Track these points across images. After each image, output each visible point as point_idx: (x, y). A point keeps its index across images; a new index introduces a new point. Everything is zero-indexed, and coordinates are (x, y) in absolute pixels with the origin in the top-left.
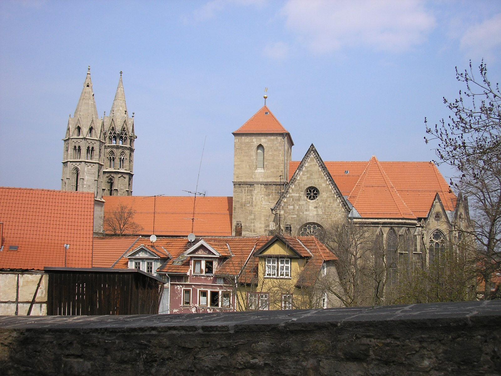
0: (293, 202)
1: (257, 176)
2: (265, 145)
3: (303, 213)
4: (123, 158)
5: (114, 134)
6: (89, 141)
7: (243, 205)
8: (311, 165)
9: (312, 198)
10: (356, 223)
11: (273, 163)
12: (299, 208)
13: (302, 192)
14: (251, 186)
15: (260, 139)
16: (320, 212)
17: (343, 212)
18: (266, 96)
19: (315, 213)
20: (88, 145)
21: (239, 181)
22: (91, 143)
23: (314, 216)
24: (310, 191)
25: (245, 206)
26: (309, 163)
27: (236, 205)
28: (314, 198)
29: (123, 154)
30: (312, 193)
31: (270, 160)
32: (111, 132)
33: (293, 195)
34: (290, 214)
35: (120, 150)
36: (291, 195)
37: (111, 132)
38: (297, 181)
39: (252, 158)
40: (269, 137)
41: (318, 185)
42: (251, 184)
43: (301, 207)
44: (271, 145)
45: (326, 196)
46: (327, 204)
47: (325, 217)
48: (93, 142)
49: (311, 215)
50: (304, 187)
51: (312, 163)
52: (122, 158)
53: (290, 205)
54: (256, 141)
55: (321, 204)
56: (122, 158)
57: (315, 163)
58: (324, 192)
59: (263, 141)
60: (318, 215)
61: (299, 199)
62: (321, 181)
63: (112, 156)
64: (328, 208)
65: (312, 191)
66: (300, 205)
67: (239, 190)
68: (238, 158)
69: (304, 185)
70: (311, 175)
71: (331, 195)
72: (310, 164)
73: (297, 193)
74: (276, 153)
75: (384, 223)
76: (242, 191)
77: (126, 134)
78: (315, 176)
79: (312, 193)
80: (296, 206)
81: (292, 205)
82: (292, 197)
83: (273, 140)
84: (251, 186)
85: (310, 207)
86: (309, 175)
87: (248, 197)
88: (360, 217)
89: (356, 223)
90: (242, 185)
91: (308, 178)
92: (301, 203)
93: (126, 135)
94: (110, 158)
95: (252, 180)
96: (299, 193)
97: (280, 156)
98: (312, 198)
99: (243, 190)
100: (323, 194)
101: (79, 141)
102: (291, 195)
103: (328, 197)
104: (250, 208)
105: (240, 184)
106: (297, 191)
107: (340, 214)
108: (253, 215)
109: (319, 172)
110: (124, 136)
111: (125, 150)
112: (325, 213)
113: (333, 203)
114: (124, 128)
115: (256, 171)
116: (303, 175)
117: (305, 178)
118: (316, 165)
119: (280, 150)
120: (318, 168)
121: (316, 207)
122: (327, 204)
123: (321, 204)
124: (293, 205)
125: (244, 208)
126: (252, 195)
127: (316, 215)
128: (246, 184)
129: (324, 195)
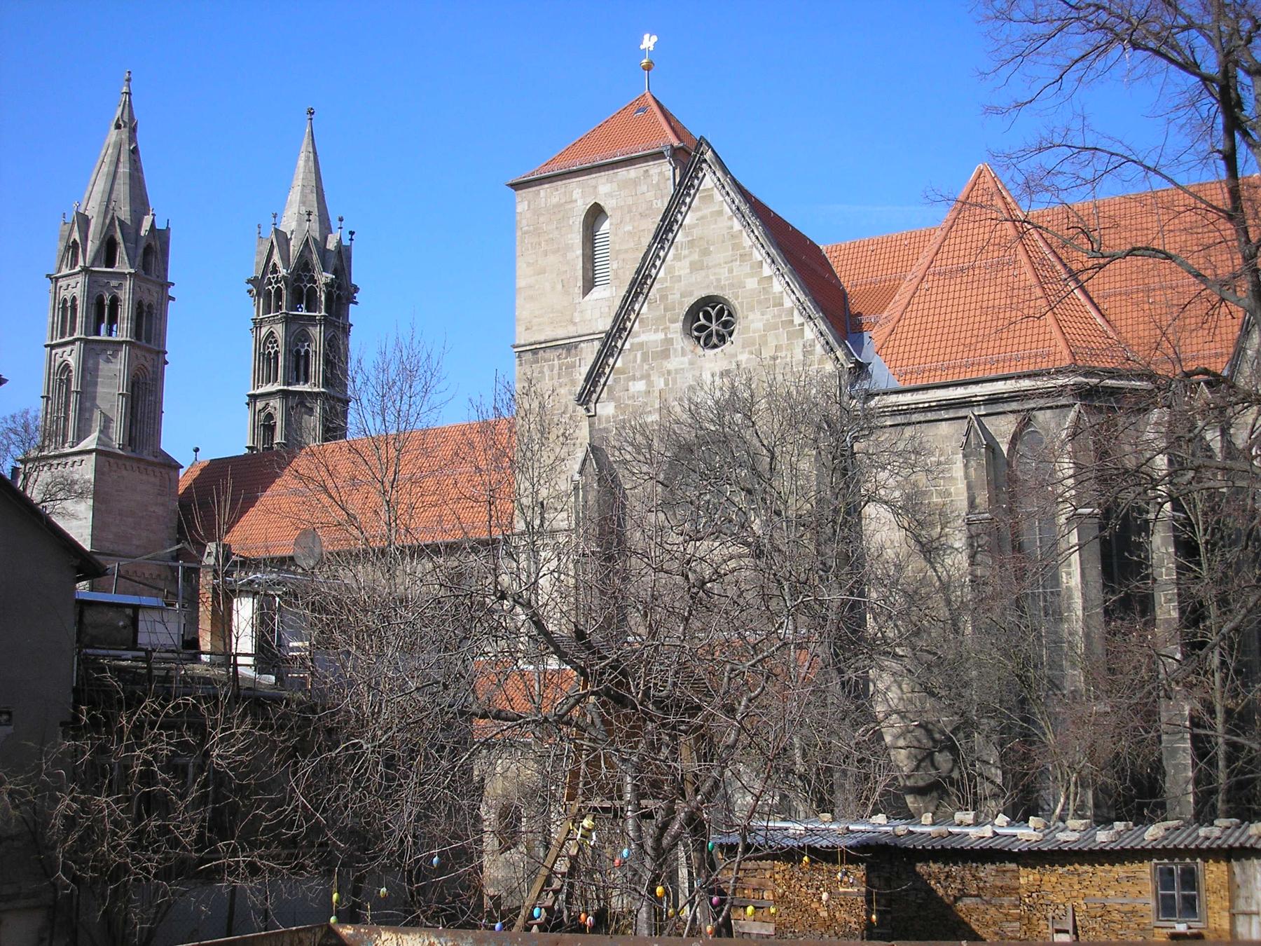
0: (646, 367)
1: (588, 315)
2: (607, 205)
8: (702, 218)
9: (715, 340)
10: (882, 415)
12: (667, 384)
14: (569, 350)
15: (595, 187)
21: (532, 340)
24: (708, 317)
26: (698, 209)
28: (722, 339)
31: (626, 251)
33: (643, 338)
36: (636, 340)
39: (570, 256)
40: (623, 173)
41: (732, 285)
44: (630, 201)
45: (760, 325)
50: (681, 303)
51: (707, 211)
52: (303, 351)
53: (634, 378)
56: (303, 351)
57: (716, 208)
58: (752, 309)
59: (604, 188)
61: (665, 354)
62: (741, 270)
65: (713, 314)
66: (669, 372)
68: (529, 264)
69: (682, 296)
70: (705, 252)
71: (780, 316)
72: (699, 214)
73: (656, 331)
75: (993, 400)
78: (720, 255)
81: (642, 378)
82: (641, 345)
83: (635, 182)
84: (569, 350)
86: (696, 257)
88: (900, 385)
90: (541, 352)
91: (695, 267)
92: (673, 363)
93: (315, 282)
95: (572, 331)
96: (666, 329)
98: (715, 340)
99: (546, 369)
101: (72, 282)
102: (636, 340)
103: (769, 327)
115: (587, 297)
118: (720, 213)
120: (729, 223)
124: (647, 377)
128: (552, 346)
129: (751, 321)
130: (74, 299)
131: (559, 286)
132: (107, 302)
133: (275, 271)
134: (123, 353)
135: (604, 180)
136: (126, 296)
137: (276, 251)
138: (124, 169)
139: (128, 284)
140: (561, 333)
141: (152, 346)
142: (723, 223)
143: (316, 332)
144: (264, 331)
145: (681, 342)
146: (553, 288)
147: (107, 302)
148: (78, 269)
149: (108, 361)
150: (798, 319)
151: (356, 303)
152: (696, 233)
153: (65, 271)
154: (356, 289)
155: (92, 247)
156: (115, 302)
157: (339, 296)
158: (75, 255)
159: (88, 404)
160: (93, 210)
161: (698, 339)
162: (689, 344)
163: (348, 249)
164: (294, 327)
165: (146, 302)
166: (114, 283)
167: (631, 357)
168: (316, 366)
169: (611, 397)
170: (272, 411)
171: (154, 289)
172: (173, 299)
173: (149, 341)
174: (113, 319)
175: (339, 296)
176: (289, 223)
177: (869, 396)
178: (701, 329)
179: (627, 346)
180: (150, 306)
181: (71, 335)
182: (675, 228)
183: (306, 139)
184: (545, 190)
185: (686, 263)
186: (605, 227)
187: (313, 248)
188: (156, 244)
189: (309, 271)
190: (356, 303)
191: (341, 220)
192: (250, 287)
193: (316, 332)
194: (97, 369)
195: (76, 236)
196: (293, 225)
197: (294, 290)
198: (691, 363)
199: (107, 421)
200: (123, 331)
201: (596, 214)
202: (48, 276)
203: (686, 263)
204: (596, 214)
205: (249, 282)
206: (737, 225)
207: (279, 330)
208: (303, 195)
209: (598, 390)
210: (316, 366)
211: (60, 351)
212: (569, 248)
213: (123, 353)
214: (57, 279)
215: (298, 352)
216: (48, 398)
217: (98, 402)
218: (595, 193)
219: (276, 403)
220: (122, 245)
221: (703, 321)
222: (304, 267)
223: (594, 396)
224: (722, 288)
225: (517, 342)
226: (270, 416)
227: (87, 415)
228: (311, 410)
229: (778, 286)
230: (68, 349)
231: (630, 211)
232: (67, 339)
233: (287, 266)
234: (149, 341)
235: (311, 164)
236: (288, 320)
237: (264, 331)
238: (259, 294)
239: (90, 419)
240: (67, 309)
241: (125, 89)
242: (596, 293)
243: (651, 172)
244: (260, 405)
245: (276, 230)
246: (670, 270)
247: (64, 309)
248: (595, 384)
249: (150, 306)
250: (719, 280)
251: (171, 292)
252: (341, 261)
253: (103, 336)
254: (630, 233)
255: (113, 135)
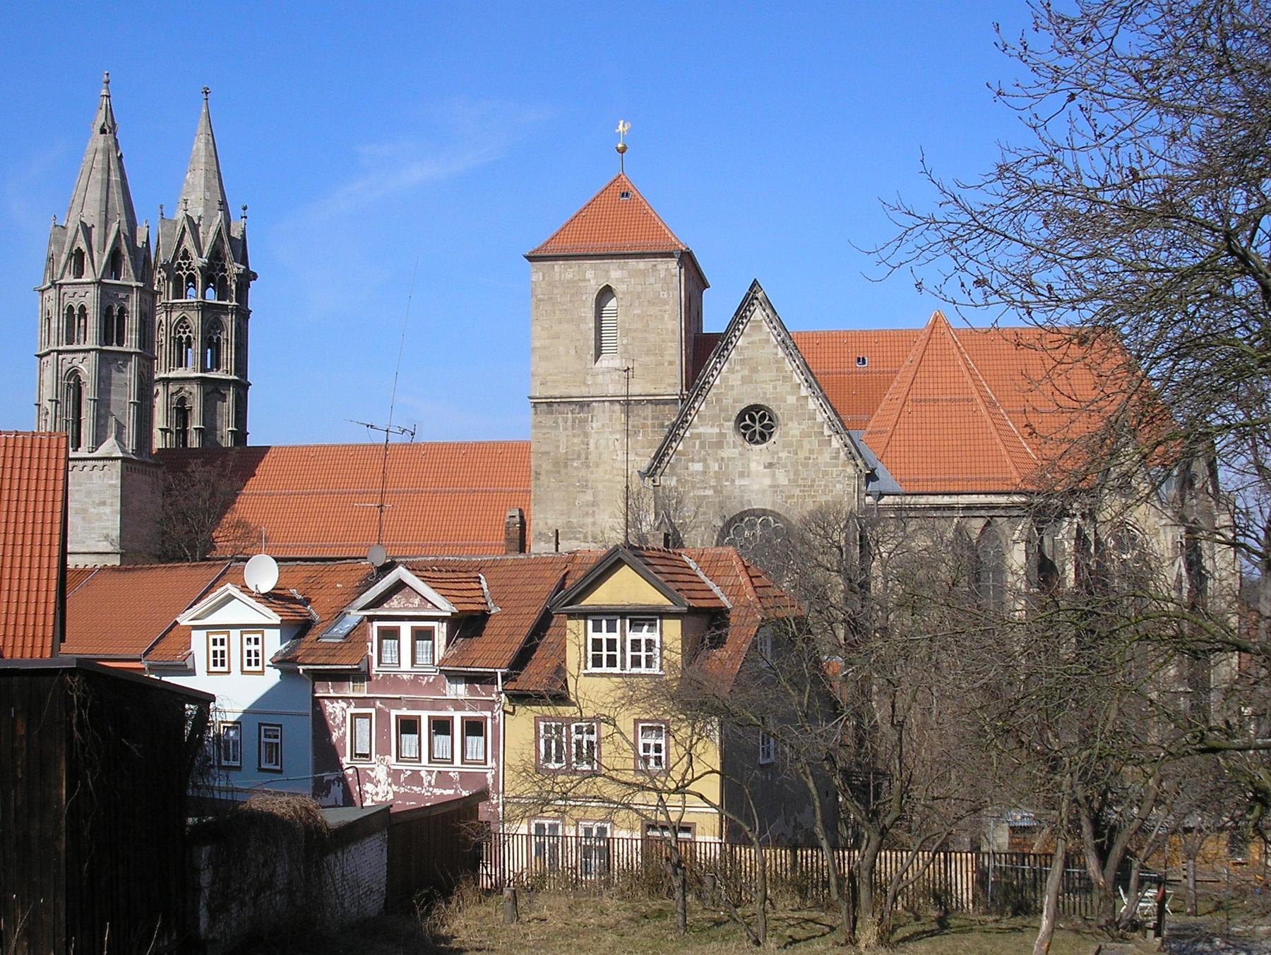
3: (733, 481)
7: (561, 464)
9: (757, 437)
10: (885, 510)
11: (645, 340)
13: (729, 420)
16: (783, 479)
17: (849, 478)
18: (620, 146)
19: (767, 481)
21: (547, 394)
23: (764, 492)
24: (752, 419)
25: (566, 466)
26: (749, 335)
27: (540, 466)
28: (764, 438)
30: (756, 423)
31: (636, 330)
33: (701, 430)
34: (693, 487)
38: (713, 390)
39: (583, 327)
40: (632, 263)
41: (775, 399)
42: (583, 405)
43: (727, 466)
44: (639, 288)
45: (797, 433)
46: (801, 455)
47: (797, 492)
49: (756, 487)
50: (734, 408)
51: (756, 338)
54: (592, 275)
55: (783, 455)
58: (791, 420)
59: (615, 273)
60: (774, 487)
61: (720, 444)
62: (783, 388)
64: (805, 465)
67: (548, 420)
68: (543, 328)
70: (754, 370)
72: (750, 339)
74: (653, 310)
75: (968, 507)
76: (556, 422)
78: (764, 376)
79: (756, 423)
80: (710, 462)
81: (699, 461)
82: (699, 436)
83: (644, 273)
85: (753, 466)
87: (575, 440)
88: (902, 490)
89: (885, 510)
92: (727, 452)
93: (225, 271)
96: (720, 426)
97: (666, 318)
99: (560, 420)
100: (790, 424)
101: (81, 291)
103: (804, 435)
104: (583, 473)
105: (550, 404)
106: (714, 420)
107: (839, 482)
108: (590, 492)
109: (777, 361)
112: (795, 481)
113: (820, 452)
116: (731, 371)
117: (735, 380)
118: (768, 341)
119: (666, 302)
121: (770, 465)
122: (801, 455)
123: (783, 455)
124: (704, 460)
125: (563, 471)
126: (586, 435)
127: (771, 486)
128: (566, 402)
129: (789, 430)
130: (83, 309)
131: (573, 352)
133: (186, 255)
134: (133, 363)
135: (615, 266)
136: (133, 305)
137: (188, 237)
138: (115, 178)
139: (135, 297)
140: (574, 391)
142: (769, 349)
143: (229, 321)
144: (176, 315)
145: (732, 436)
146: (568, 352)
147: (116, 313)
149: (120, 371)
150: (827, 432)
152: (747, 354)
153: (71, 279)
155: (101, 259)
156: (122, 311)
159: (103, 411)
160: (92, 215)
161: (744, 435)
162: (739, 439)
164: (208, 315)
166: (121, 295)
167: (691, 444)
168: (228, 354)
169: (673, 473)
170: (187, 395)
176: (197, 211)
177: (882, 495)
178: (746, 427)
179: (687, 434)
182: (730, 347)
183: (203, 121)
184: (558, 266)
185: (739, 375)
186: (612, 304)
187: (225, 239)
189: (220, 260)
193: (229, 321)
194: (110, 378)
195: (84, 247)
196: (200, 211)
198: (741, 454)
199: (120, 428)
200: (131, 344)
201: (606, 293)
203: (739, 375)
204: (606, 293)
206: (781, 354)
207: (195, 319)
208: (207, 180)
209: (663, 465)
210: (228, 354)
211: (69, 356)
212: (583, 320)
213: (133, 363)
214: (61, 285)
215: (211, 338)
216: (57, 402)
217: (112, 410)
218: (608, 279)
219: (195, 389)
220: (127, 257)
221: (748, 422)
222: (216, 254)
223: (659, 471)
224: (767, 400)
225: (532, 394)
226: (182, 400)
227: (102, 422)
228: (225, 396)
229: (812, 404)
230: (81, 355)
231: (639, 297)
235: (211, 147)
236: (205, 308)
237: (176, 315)
238: (168, 278)
239: (106, 426)
240: (74, 317)
241: (104, 92)
242: (605, 362)
243: (659, 267)
244: (173, 388)
245: (189, 218)
246: (724, 380)
248: (660, 461)
250: (765, 394)
252: (240, 249)
253: (115, 348)
254: (638, 315)
255: (99, 141)
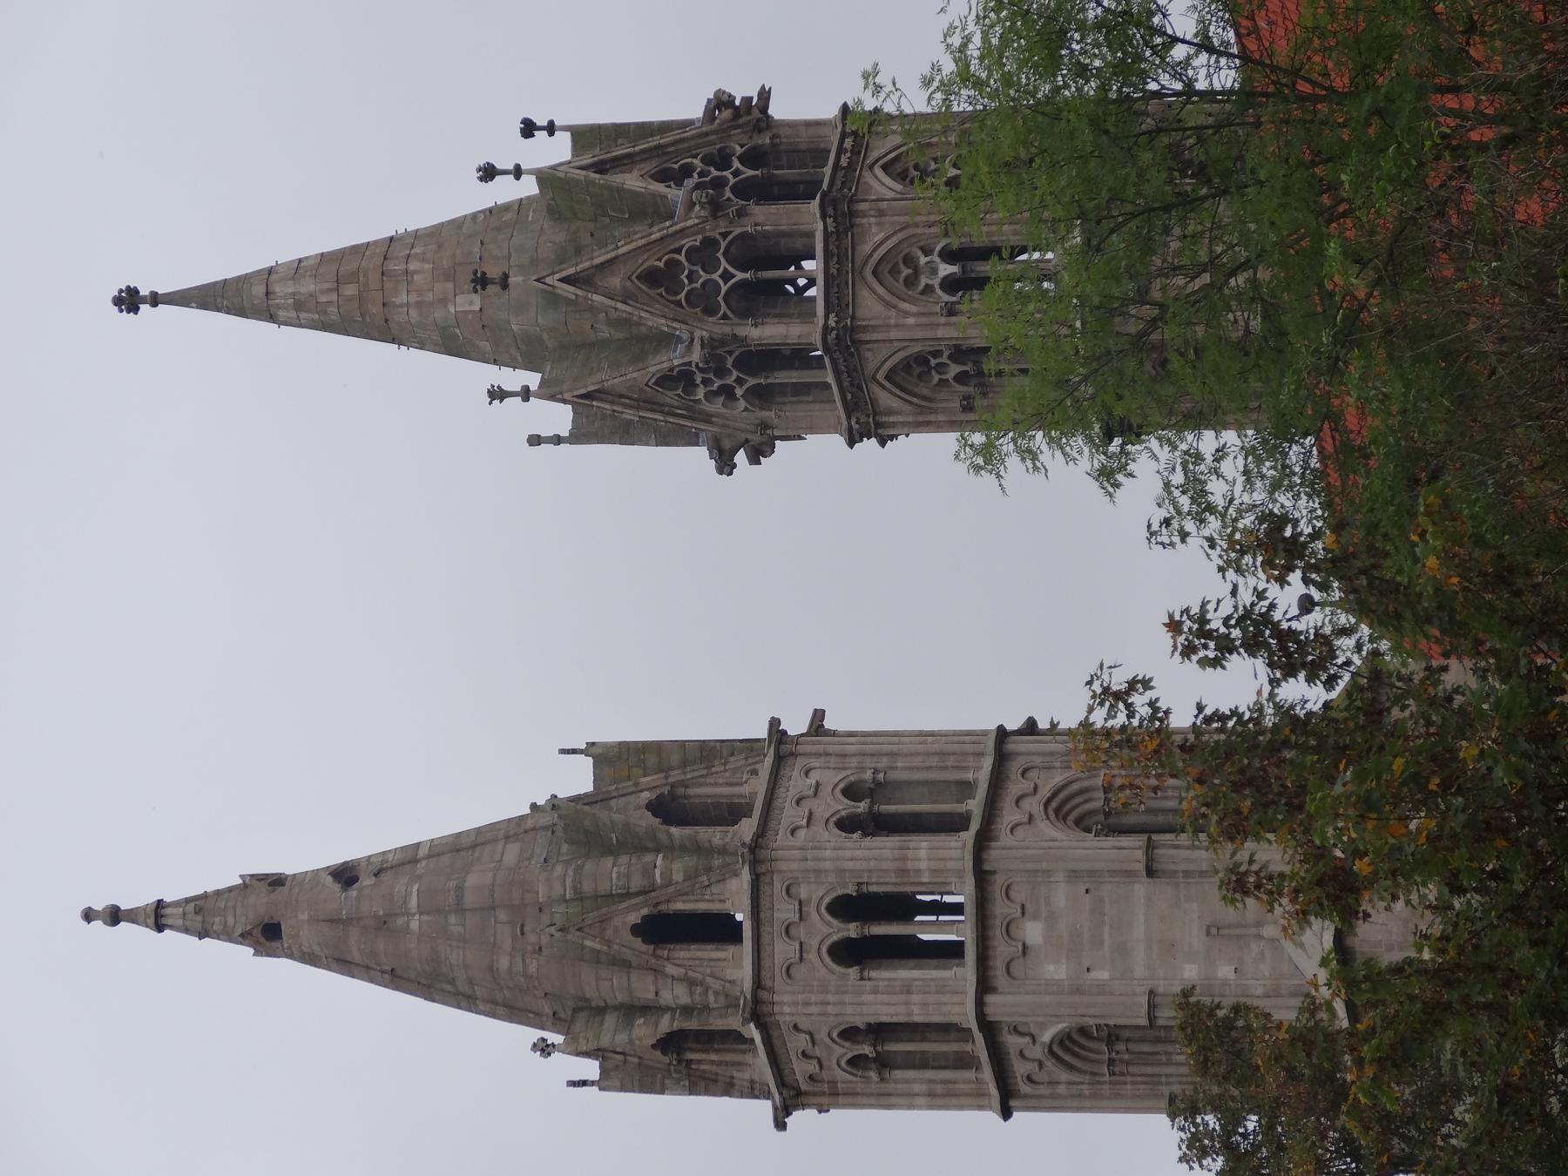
4: (949, 256)
5: (721, 372)
6: (781, 951)
20: (821, 968)
22: (801, 931)
29: (909, 260)
32: (710, 396)
35: (870, 305)
37: (710, 396)
48: (784, 911)
52: (946, 270)
56: (946, 270)
63: (941, 367)
77: (704, 254)
93: (710, 243)
94: (961, 378)
110: (727, 275)
111: (866, 248)
114: (651, 277)
132: (852, 930)
141: (983, 775)
147: (852, 930)
148: (753, 1032)
151: (765, 95)
154: (721, 102)
157: (753, 158)
158: (708, 1039)
163: (584, 137)
165: (844, 806)
171: (796, 782)
172: (819, 715)
173: (966, 789)
174: (903, 906)
175: (751, 158)
180: (851, 792)
181: (964, 1033)
188: (650, 785)
189: (673, 264)
190: (765, 95)
191: (489, 173)
192: (741, 457)
197: (744, 314)
202: (780, 1125)
205: (725, 465)
215: (950, 285)
232: (980, 1048)
233: (665, 340)
234: (966, 789)
237: (886, 399)
247: (884, 1063)
249: (851, 792)
251: (796, 725)
